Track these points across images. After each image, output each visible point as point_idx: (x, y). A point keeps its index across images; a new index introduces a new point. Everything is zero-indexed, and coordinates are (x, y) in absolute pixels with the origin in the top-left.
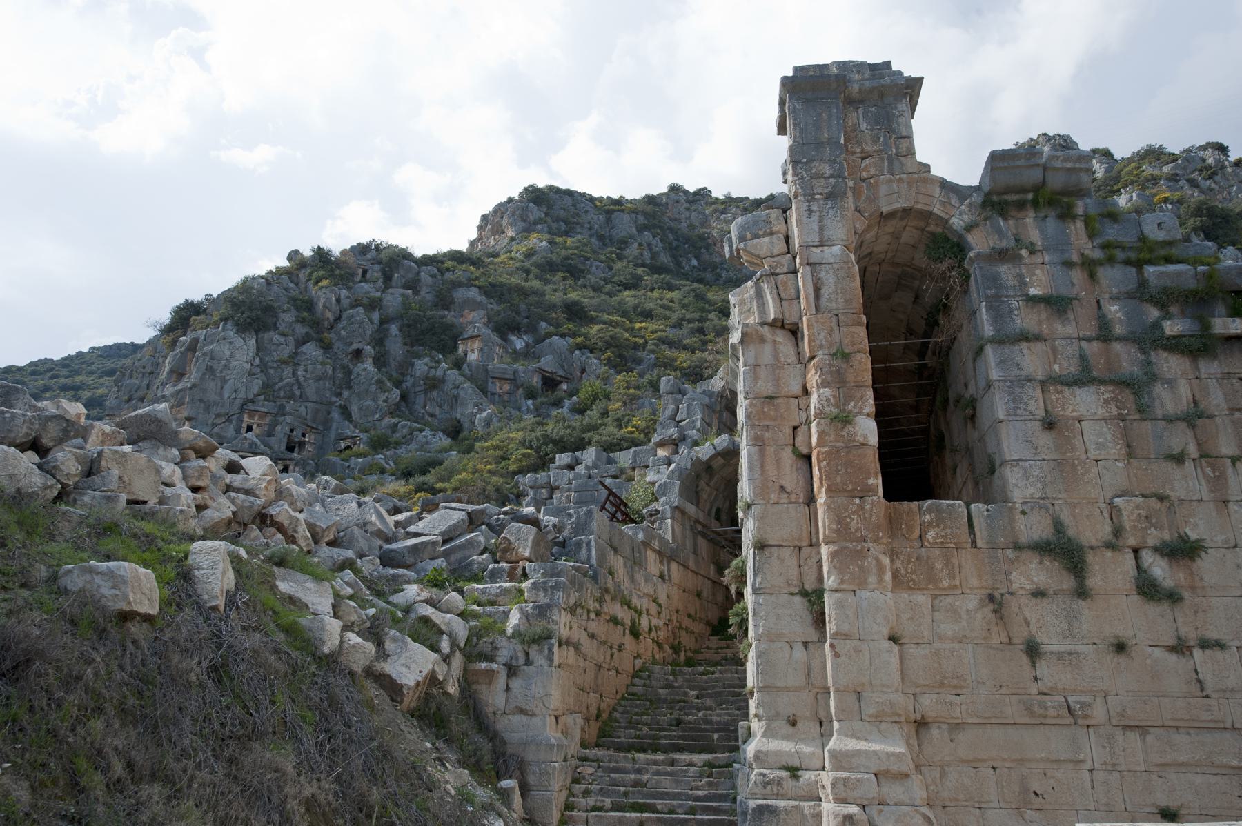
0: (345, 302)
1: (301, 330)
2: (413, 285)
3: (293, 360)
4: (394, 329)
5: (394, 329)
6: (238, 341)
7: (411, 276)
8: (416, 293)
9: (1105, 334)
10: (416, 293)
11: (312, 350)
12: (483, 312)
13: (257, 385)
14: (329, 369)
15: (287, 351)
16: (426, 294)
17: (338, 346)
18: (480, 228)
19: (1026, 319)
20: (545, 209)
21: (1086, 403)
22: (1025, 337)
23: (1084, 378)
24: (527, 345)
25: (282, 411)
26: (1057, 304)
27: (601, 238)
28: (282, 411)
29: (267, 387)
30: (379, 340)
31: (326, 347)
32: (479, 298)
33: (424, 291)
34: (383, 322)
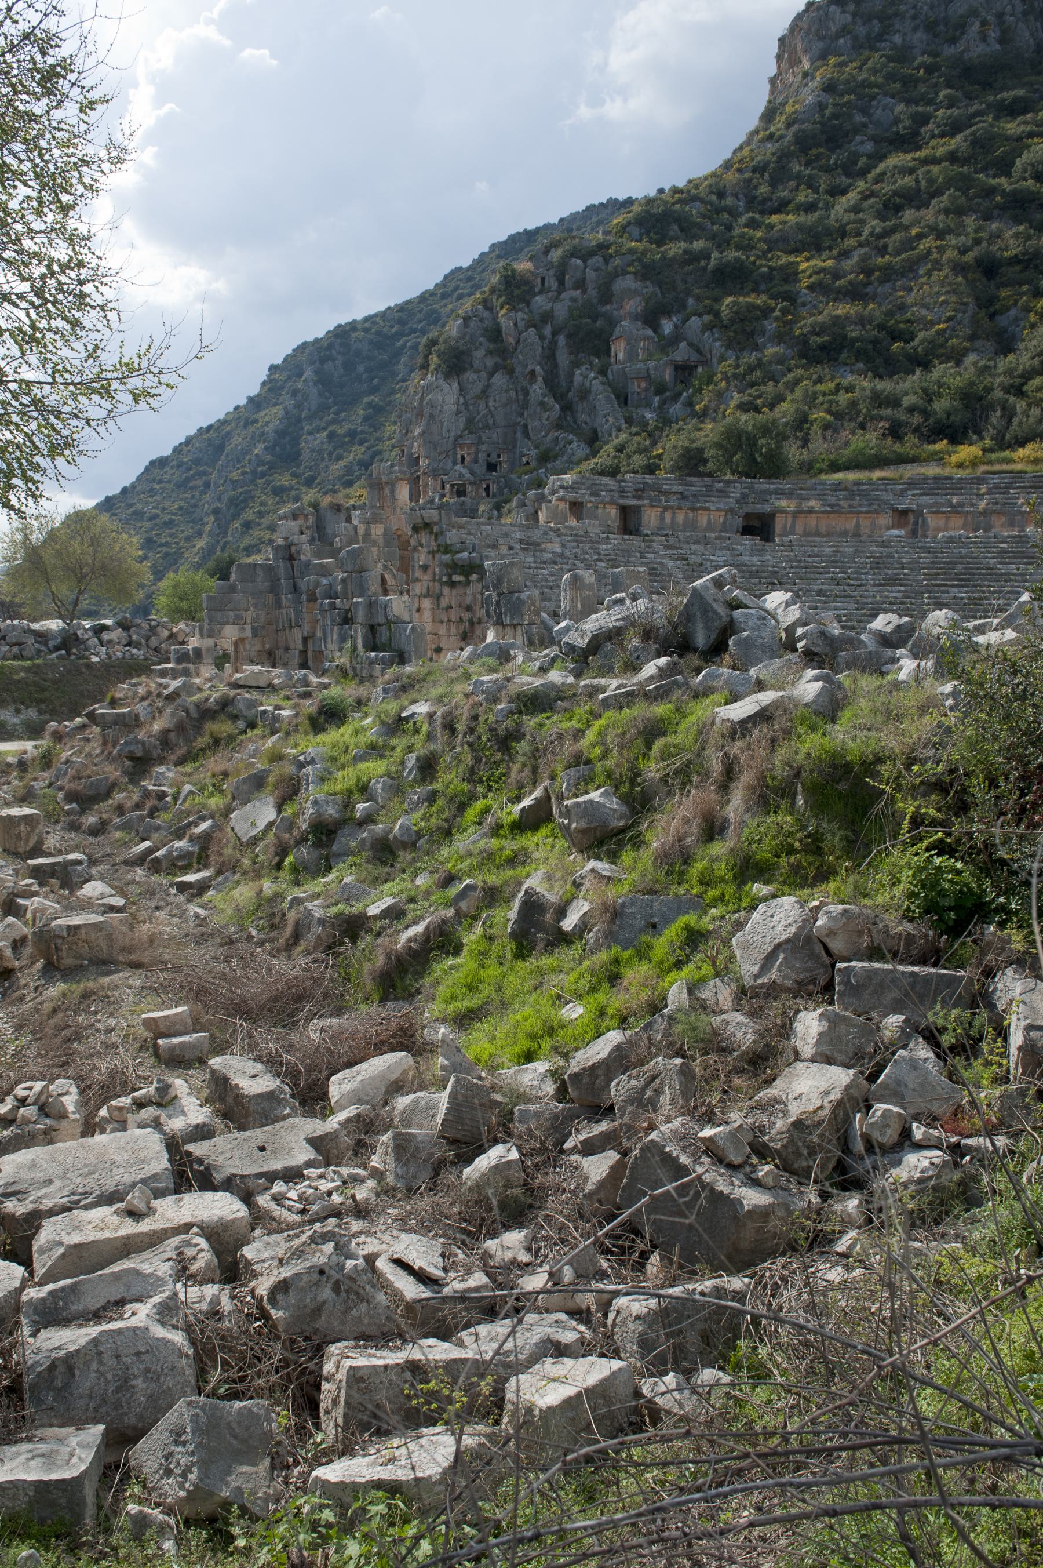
0: (521, 325)
1: (490, 362)
2: (580, 284)
3: (484, 393)
4: (562, 340)
5: (562, 340)
6: (446, 386)
7: (579, 274)
8: (584, 292)
9: (434, 580)
10: (584, 292)
11: (500, 380)
12: (638, 299)
13: (462, 420)
14: (513, 394)
15: (479, 387)
16: (592, 292)
17: (518, 369)
18: (779, 58)
19: (418, 574)
20: (851, 7)
21: (427, 604)
22: (418, 580)
23: (427, 595)
24: (676, 326)
25: (480, 442)
26: (425, 568)
27: (930, 27)
28: (480, 442)
29: (470, 421)
30: (550, 356)
31: (511, 372)
32: (633, 286)
33: (590, 287)
34: (554, 334)
